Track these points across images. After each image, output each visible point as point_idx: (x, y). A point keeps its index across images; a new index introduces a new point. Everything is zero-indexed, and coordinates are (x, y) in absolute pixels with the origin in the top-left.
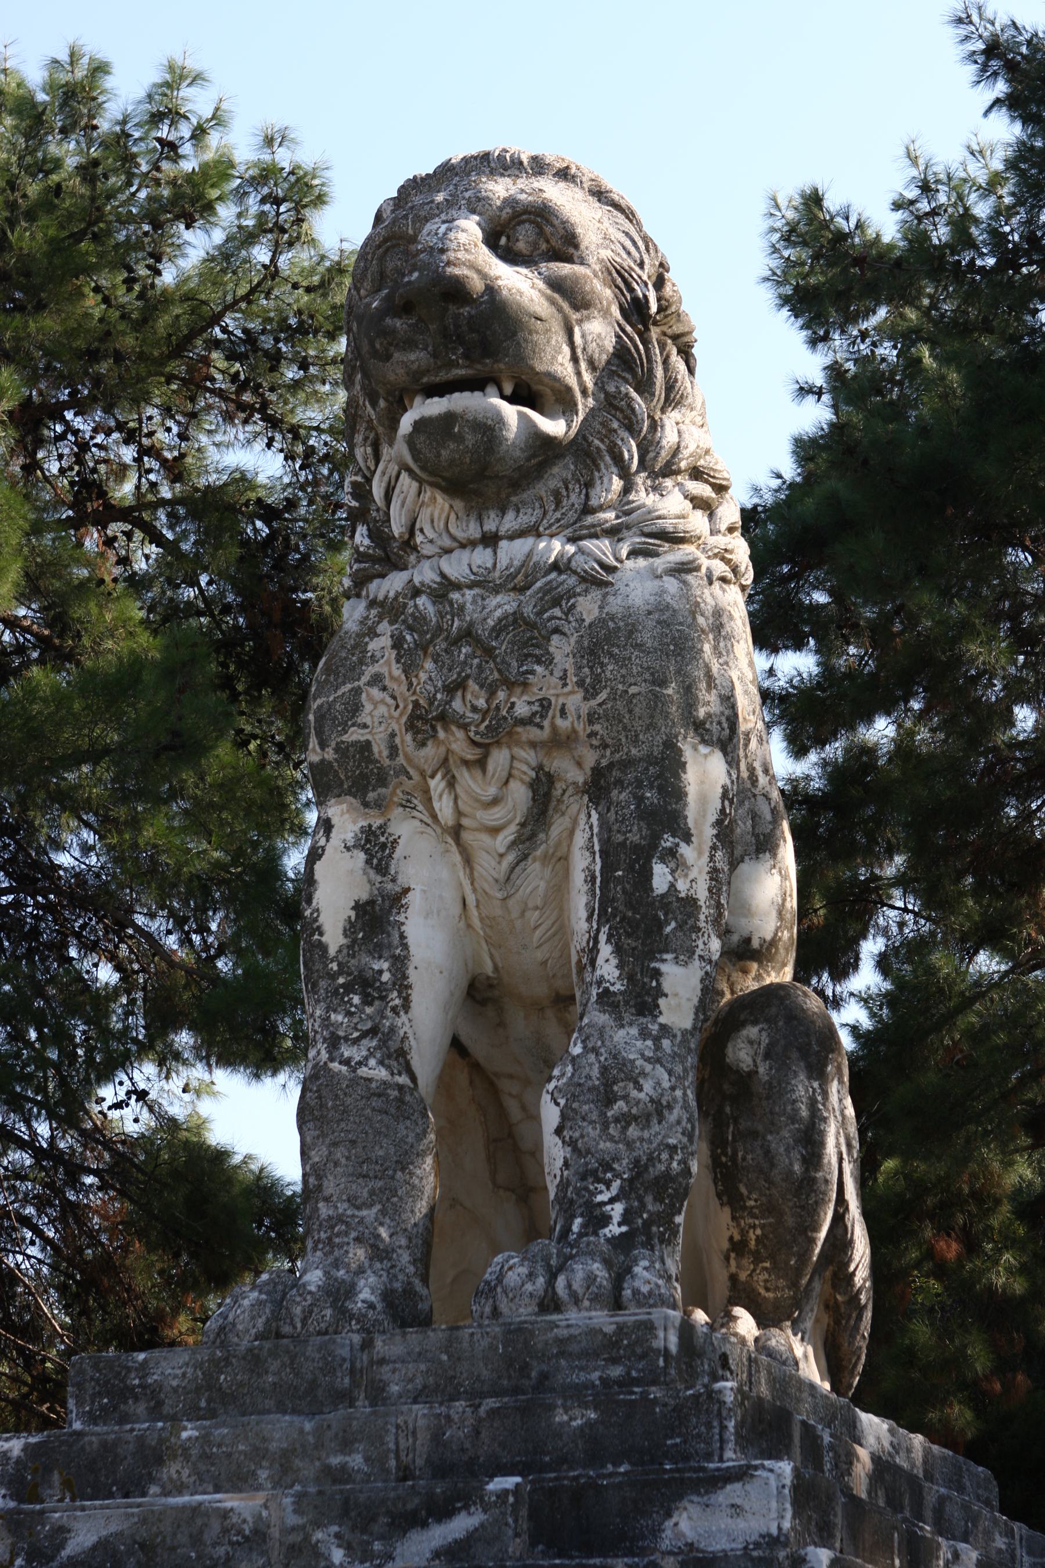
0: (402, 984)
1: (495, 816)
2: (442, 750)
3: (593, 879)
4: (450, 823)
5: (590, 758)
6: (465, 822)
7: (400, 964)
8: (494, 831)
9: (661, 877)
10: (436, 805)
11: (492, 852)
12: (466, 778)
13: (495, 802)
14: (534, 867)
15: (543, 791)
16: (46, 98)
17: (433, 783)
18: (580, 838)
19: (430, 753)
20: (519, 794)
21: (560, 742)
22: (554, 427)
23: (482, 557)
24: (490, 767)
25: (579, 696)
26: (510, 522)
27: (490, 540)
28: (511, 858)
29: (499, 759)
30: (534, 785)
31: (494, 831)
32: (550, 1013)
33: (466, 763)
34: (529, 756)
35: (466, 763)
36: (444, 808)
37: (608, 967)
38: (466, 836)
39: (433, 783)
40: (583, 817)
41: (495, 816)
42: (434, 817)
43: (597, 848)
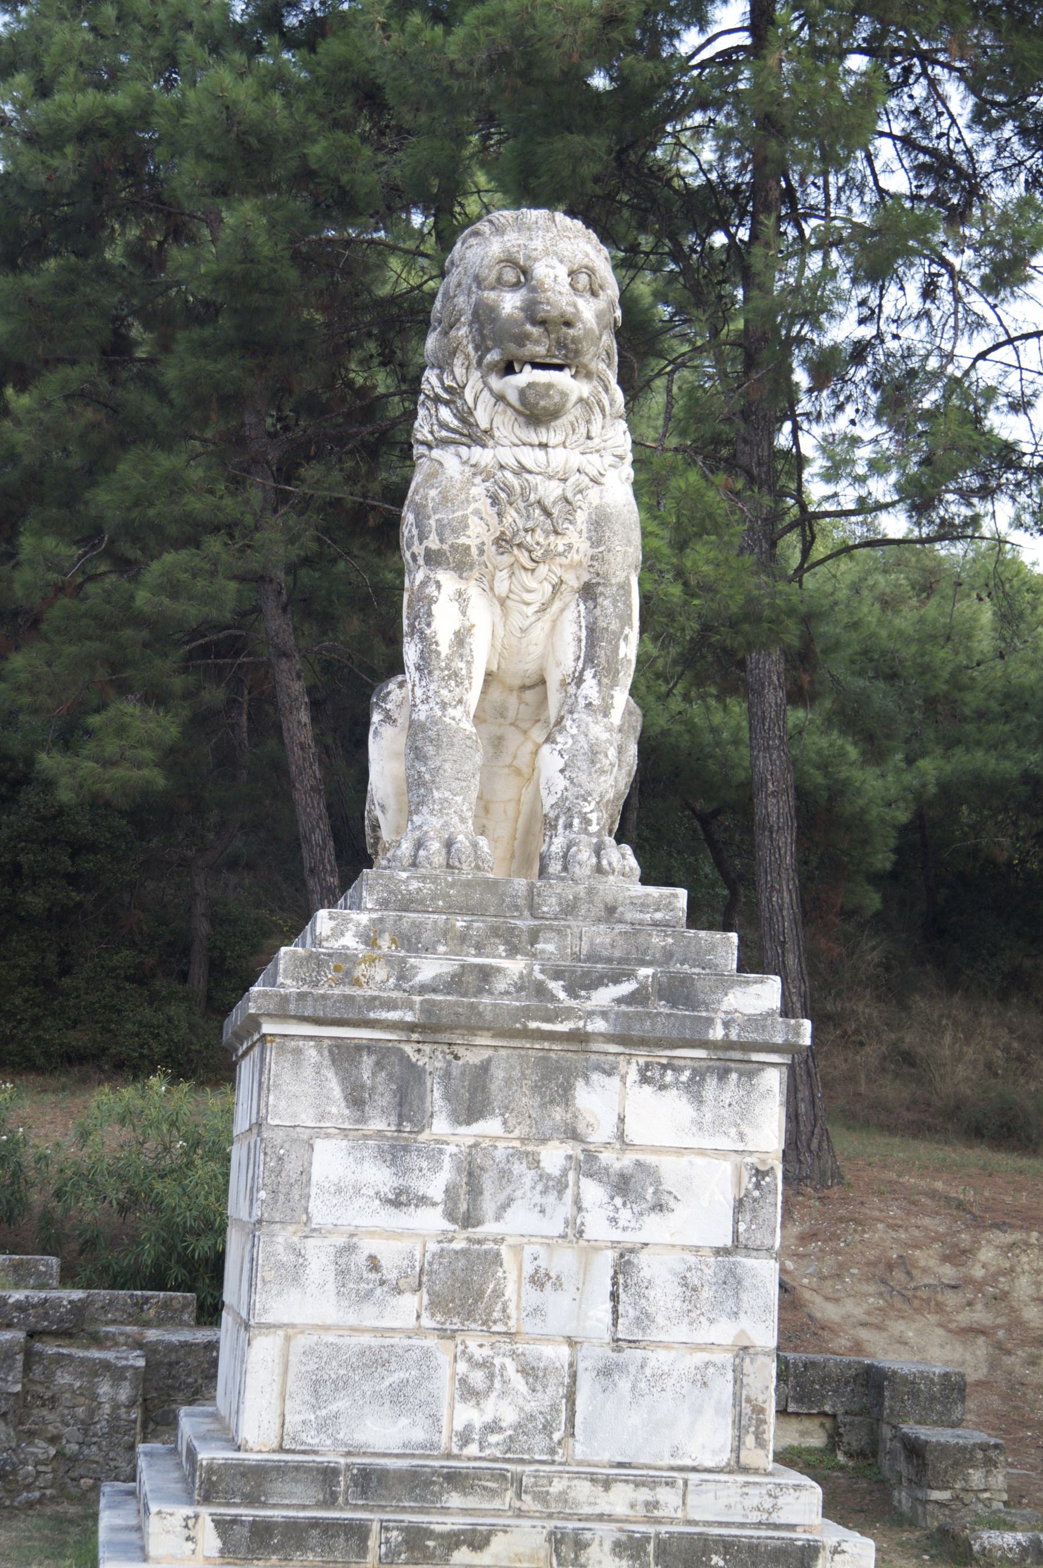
2: (512, 559)
3: (580, 640)
4: (504, 595)
6: (511, 596)
8: (528, 604)
10: (496, 584)
14: (540, 624)
17: (499, 574)
19: (506, 559)
24: (536, 573)
25: (588, 544)
28: (533, 619)
29: (543, 569)
31: (528, 604)
32: (515, 693)
33: (525, 569)
34: (559, 571)
35: (525, 569)
36: (502, 586)
38: (509, 602)
39: (499, 574)
40: (573, 604)
42: (492, 589)
43: (583, 624)
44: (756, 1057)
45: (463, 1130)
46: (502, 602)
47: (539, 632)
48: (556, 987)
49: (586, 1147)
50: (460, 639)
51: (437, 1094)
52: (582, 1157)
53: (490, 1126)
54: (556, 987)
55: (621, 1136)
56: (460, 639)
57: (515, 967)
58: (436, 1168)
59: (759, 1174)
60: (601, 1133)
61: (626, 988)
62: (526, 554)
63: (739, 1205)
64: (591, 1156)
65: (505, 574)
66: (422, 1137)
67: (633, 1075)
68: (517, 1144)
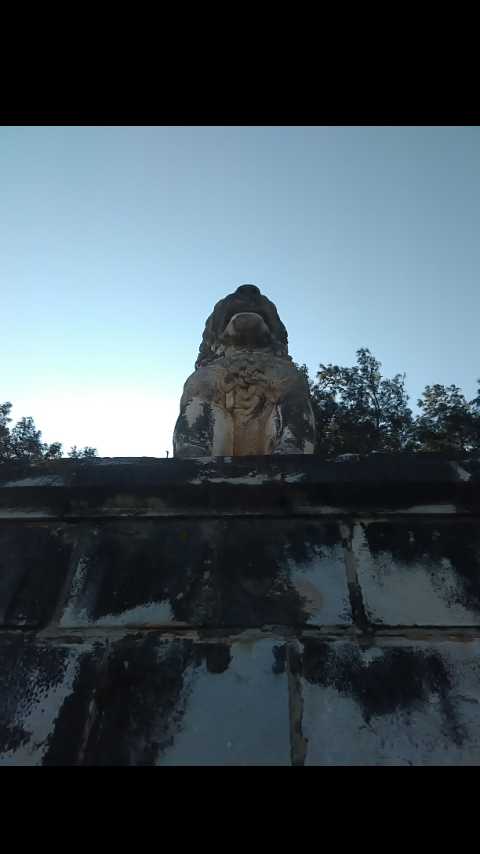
1: (247, 404)
5: (279, 395)
8: (246, 408)
11: (243, 416)
12: (240, 392)
13: (248, 400)
19: (230, 386)
20: (256, 400)
21: (271, 389)
29: (252, 389)
30: (261, 398)
36: (230, 402)
40: (274, 410)
41: (247, 404)
42: (225, 405)
45: (108, 620)
46: (231, 411)
47: (255, 426)
49: (306, 633)
51: (79, 575)
52: (301, 648)
58: (53, 676)
62: (242, 380)
64: (317, 649)
65: (231, 394)
66: (42, 635)
67: (359, 538)
68: (194, 636)
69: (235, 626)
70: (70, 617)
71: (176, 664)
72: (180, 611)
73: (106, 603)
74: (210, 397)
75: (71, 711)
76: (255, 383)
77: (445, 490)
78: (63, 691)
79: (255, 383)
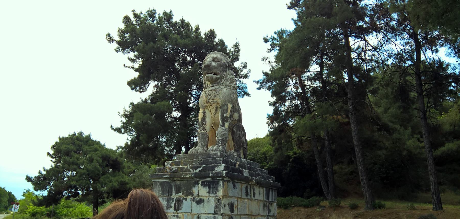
0: (206, 124)
7: (206, 122)
9: (225, 115)
11: (213, 113)
15: (217, 108)
16: (204, 37)
18: (220, 111)
19: (208, 105)
20: (215, 108)
21: (218, 104)
22: (218, 76)
23: (212, 88)
26: (215, 85)
27: (213, 86)
29: (213, 105)
37: (221, 123)
44: (218, 179)
48: (191, 170)
50: (204, 119)
53: (180, 194)
54: (191, 170)
55: (198, 194)
56: (204, 119)
57: (186, 167)
58: (173, 201)
59: (219, 200)
60: (195, 194)
61: (201, 169)
63: (216, 205)
64: (194, 198)
67: (200, 184)
69: (187, 196)
70: (174, 194)
71: (183, 200)
72: (183, 194)
73: (177, 193)
74: (204, 108)
75: (175, 204)
76: (213, 103)
77: (209, 177)
78: (174, 203)
79: (213, 103)
